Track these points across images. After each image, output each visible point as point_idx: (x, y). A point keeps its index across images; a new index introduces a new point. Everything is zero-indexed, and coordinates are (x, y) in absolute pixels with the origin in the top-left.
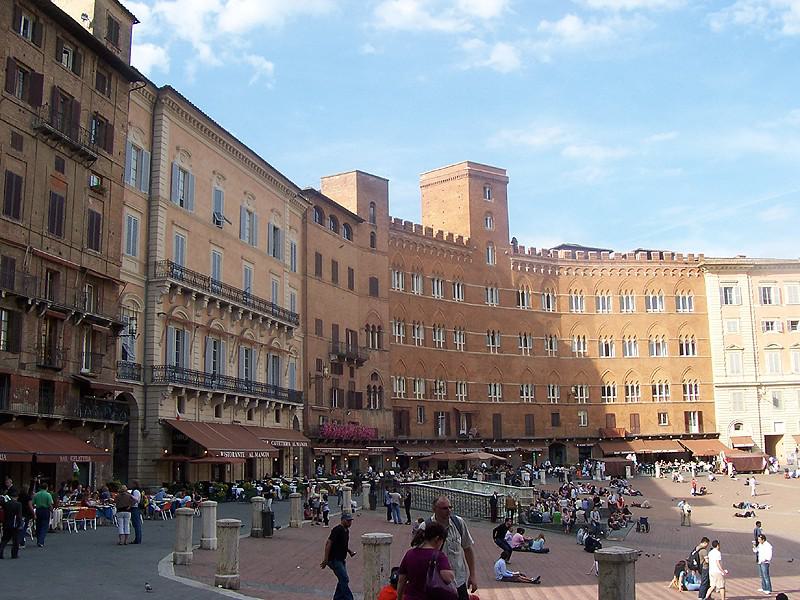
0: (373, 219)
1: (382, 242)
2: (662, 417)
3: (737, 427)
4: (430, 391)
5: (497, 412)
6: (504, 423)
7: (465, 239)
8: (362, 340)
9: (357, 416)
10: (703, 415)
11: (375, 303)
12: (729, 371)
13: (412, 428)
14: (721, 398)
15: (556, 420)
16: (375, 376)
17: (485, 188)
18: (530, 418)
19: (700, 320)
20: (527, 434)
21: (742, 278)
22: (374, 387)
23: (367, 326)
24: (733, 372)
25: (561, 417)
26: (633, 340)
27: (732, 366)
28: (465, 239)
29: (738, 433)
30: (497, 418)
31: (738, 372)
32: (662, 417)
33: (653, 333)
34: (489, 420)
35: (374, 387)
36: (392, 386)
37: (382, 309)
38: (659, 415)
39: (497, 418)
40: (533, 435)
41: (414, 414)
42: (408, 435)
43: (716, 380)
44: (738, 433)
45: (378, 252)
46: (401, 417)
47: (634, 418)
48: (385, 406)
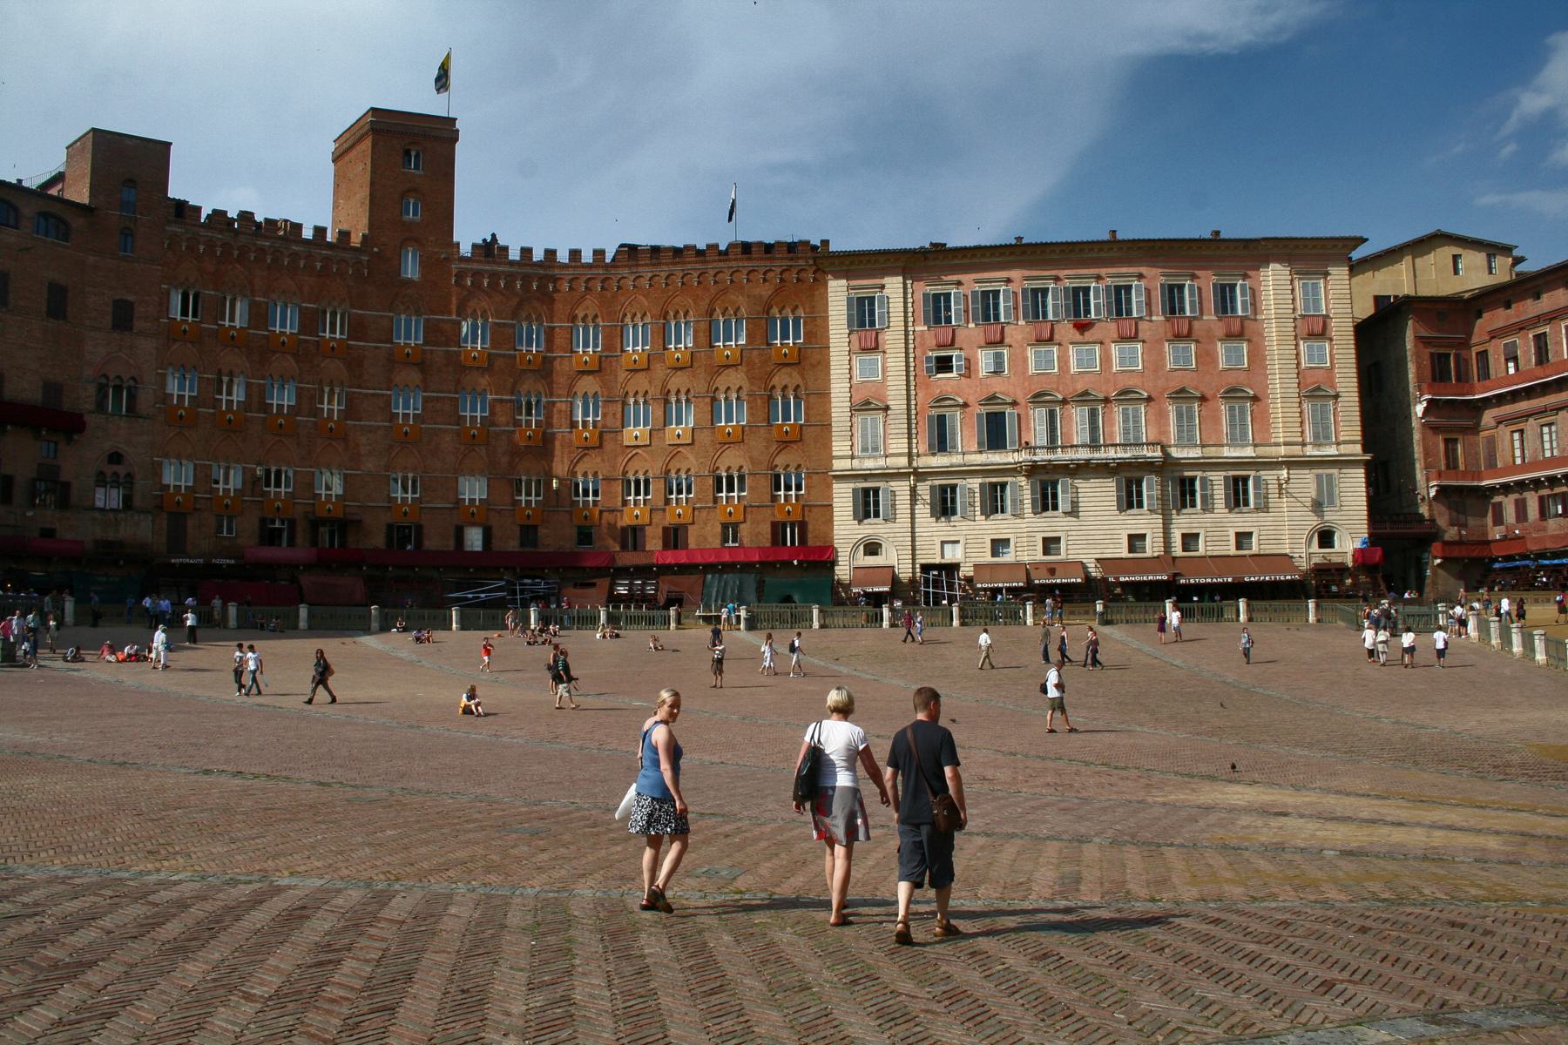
3: (872, 548)
4: (253, 484)
7: (356, 240)
10: (810, 527)
14: (842, 498)
16: (116, 458)
17: (407, 153)
19: (810, 360)
21: (893, 286)
22: (116, 474)
23: (105, 376)
24: (865, 449)
26: (683, 398)
27: (864, 436)
28: (356, 240)
29: (871, 561)
31: (875, 449)
32: (730, 529)
36: (157, 471)
38: (725, 526)
43: (839, 465)
44: (871, 561)
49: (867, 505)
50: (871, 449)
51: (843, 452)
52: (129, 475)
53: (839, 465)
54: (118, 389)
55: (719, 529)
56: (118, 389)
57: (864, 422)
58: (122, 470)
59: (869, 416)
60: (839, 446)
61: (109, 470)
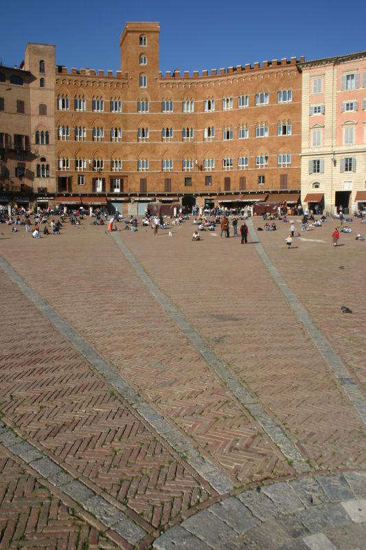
0: (42, 70)
1: (50, 81)
2: (262, 179)
5: (144, 178)
6: (148, 184)
8: (33, 140)
9: (26, 182)
11: (44, 119)
12: (312, 143)
13: (73, 188)
14: (305, 165)
15: (188, 181)
17: (141, 39)
18: (168, 182)
20: (165, 191)
22: (43, 165)
23: (38, 132)
24: (314, 144)
25: (193, 180)
30: (143, 182)
32: (262, 179)
33: (259, 120)
34: (137, 183)
35: (43, 165)
37: (49, 123)
38: (260, 177)
39: (143, 182)
40: (170, 191)
41: (75, 181)
42: (70, 189)
45: (47, 89)
46: (63, 183)
47: (243, 181)
48: (50, 175)
49: (316, 167)
50: (317, 143)
51: (307, 147)
52: (48, 166)
53: (304, 152)
54: (42, 136)
55: (257, 178)
56: (42, 136)
57: (314, 133)
58: (45, 164)
59: (316, 130)
60: (304, 144)
61: (41, 163)
